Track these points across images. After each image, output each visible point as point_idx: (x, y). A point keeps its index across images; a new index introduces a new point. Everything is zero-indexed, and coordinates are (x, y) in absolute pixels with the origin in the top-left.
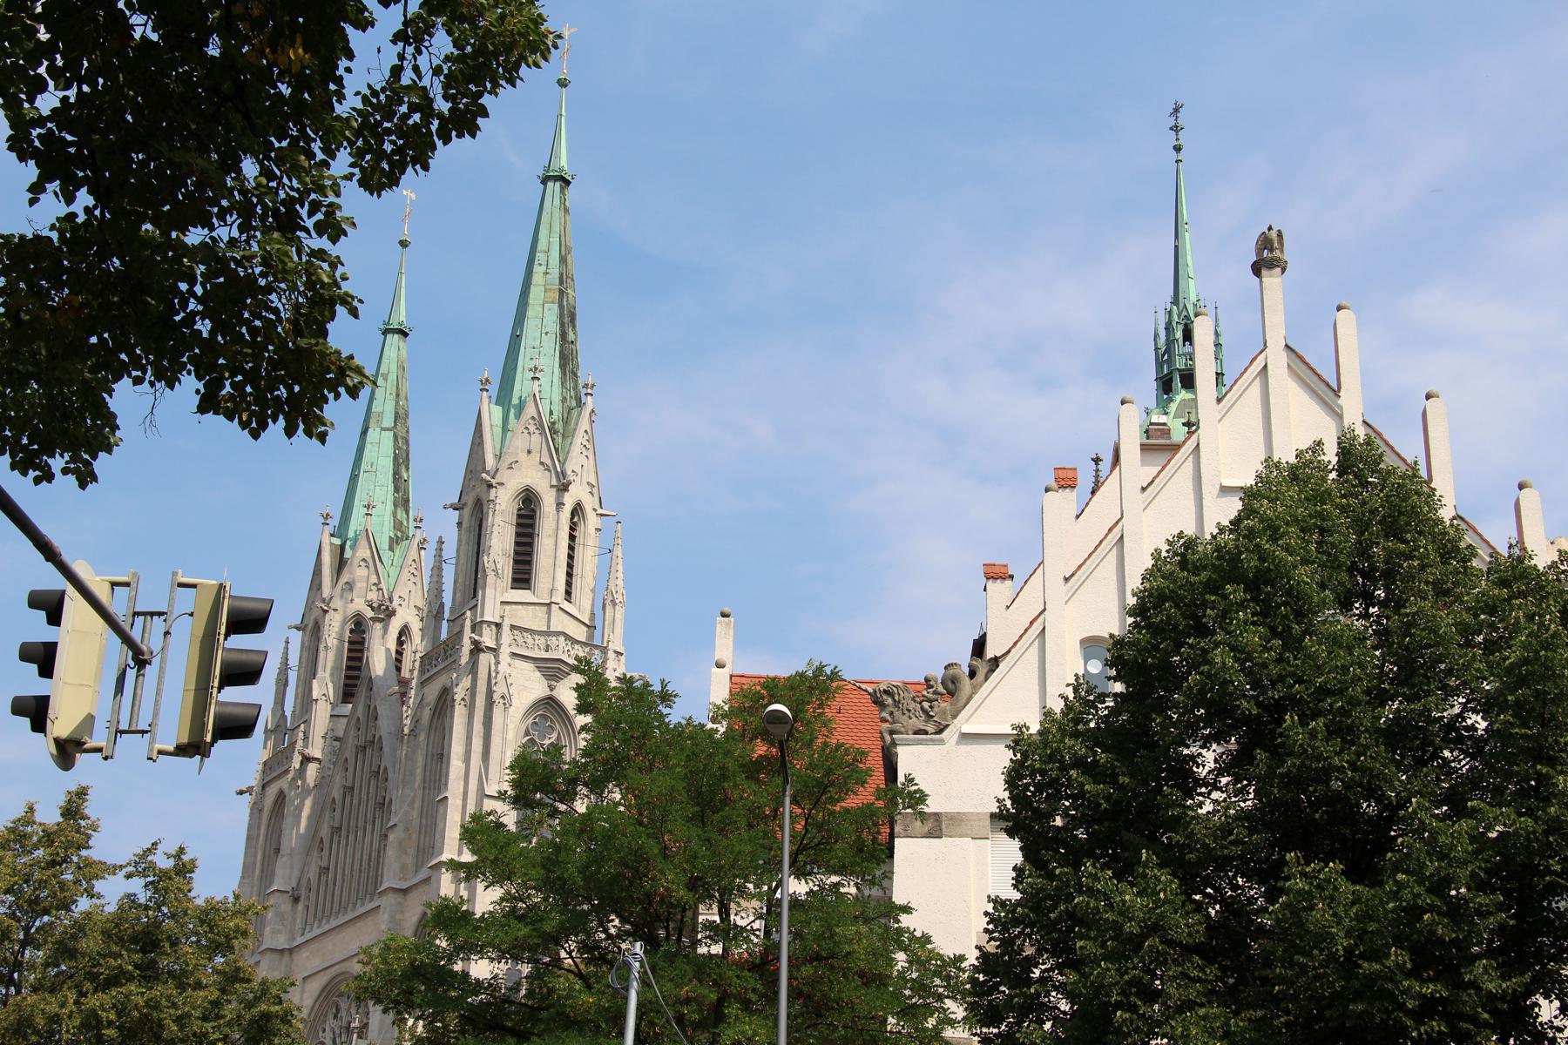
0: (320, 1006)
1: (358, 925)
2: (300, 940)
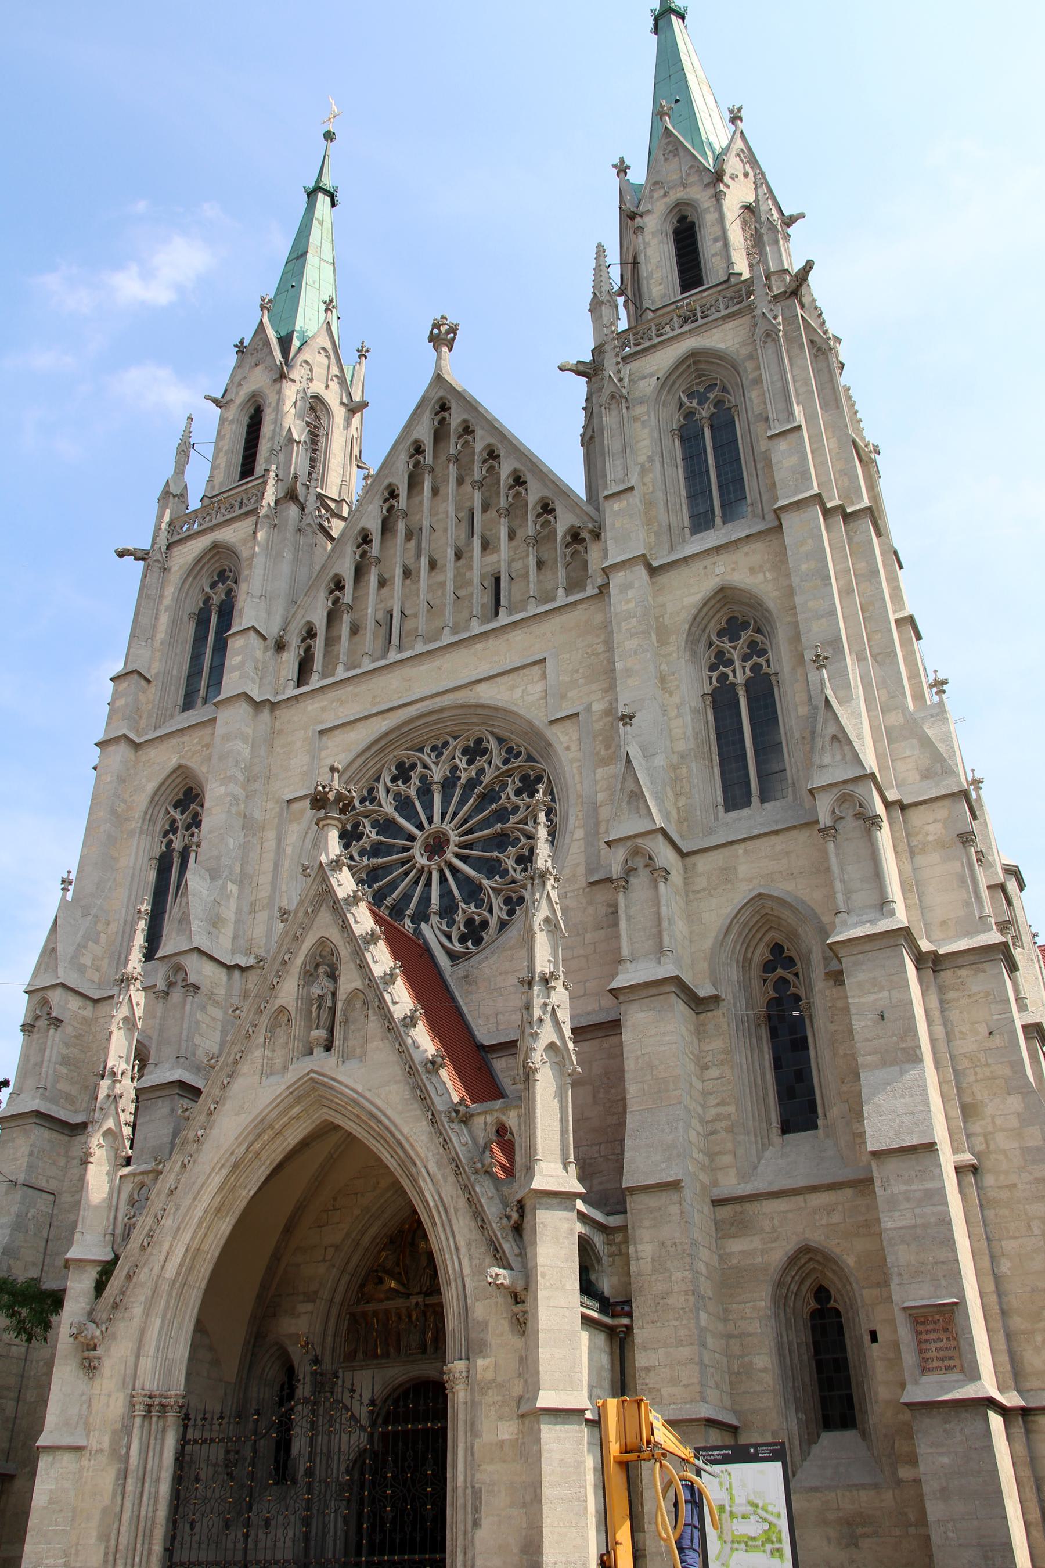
0: (365, 763)
1: (479, 646)
2: (291, 692)
